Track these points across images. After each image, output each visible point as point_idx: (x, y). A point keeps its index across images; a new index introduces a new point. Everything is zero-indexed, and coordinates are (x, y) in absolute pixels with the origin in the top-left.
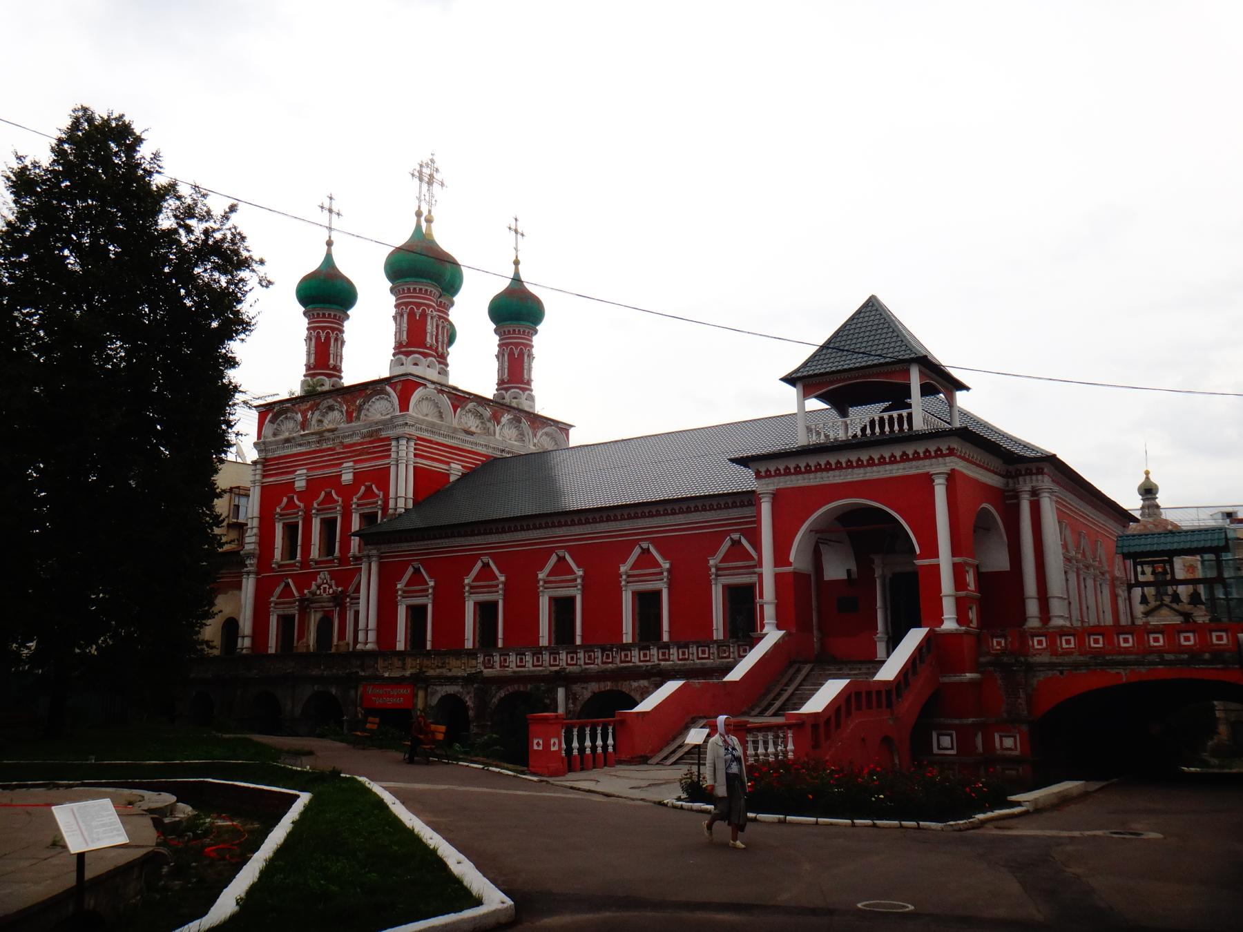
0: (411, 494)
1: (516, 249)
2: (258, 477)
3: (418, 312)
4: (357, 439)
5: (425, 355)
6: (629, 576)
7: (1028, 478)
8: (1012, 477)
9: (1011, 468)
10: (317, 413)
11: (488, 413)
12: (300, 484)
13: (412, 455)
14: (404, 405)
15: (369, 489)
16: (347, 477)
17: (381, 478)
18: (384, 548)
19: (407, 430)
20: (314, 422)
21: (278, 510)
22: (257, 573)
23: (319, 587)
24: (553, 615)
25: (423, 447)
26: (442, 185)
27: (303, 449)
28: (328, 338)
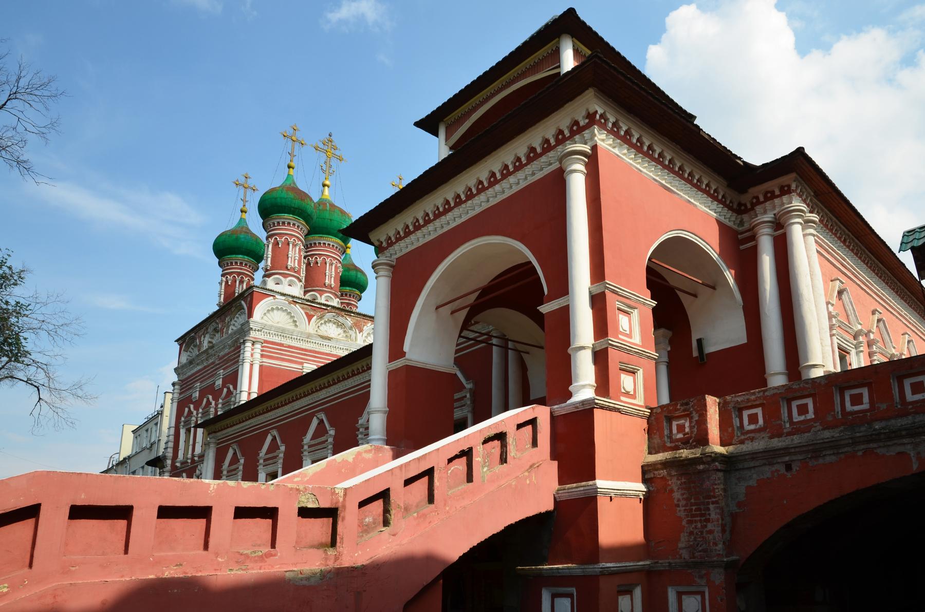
7: (768, 204)
8: (746, 211)
9: (746, 199)
13: (257, 356)
14: (250, 315)
15: (229, 388)
16: (219, 382)
18: (220, 434)
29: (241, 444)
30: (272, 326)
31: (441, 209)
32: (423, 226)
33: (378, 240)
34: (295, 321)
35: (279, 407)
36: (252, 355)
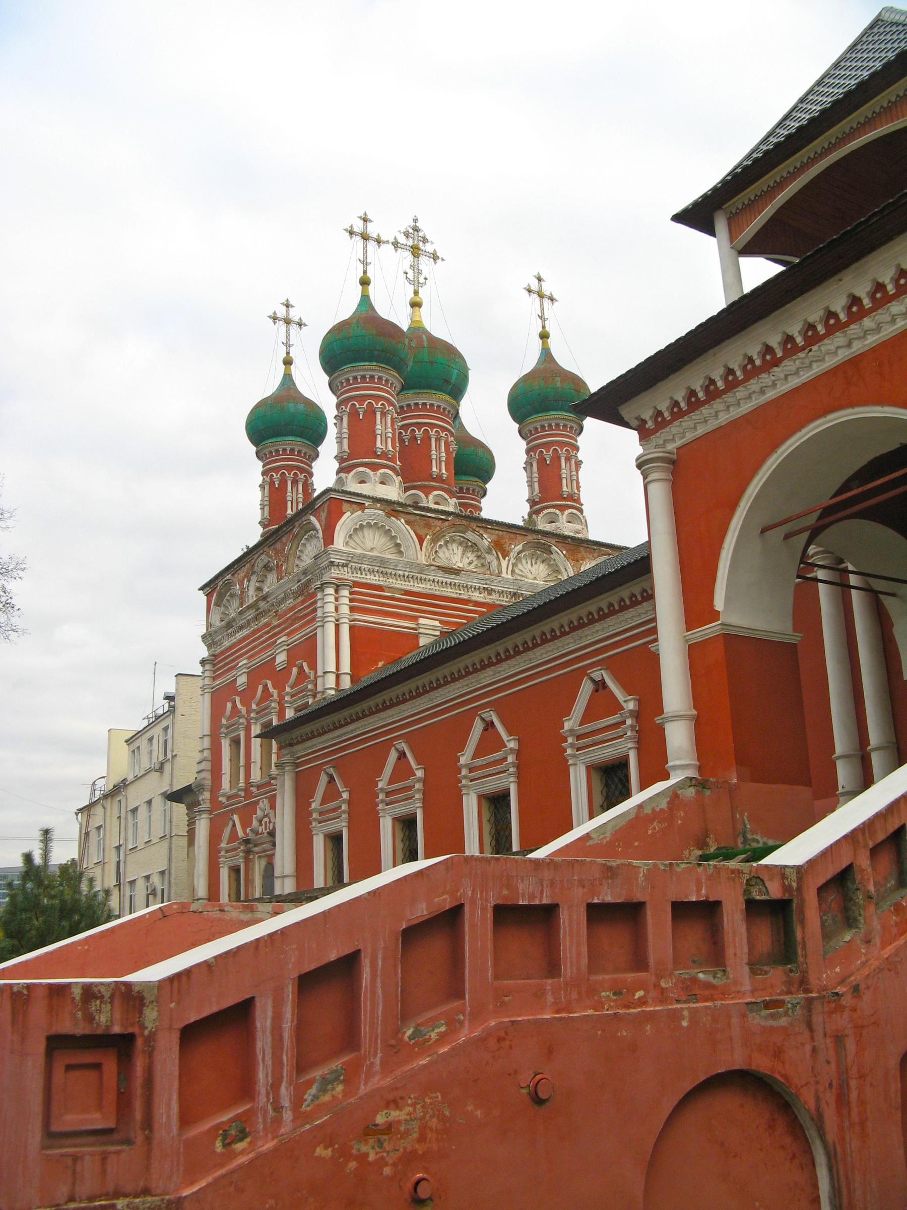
0: (346, 667)
1: (542, 317)
2: (207, 681)
3: (361, 408)
4: (290, 602)
5: (374, 467)
6: (579, 737)
10: (254, 578)
11: (486, 541)
12: (242, 680)
13: (345, 610)
14: (329, 539)
16: (281, 658)
17: (307, 651)
19: (334, 573)
20: (252, 592)
21: (224, 721)
22: (210, 812)
23: (260, 821)
24: (487, 827)
25: (364, 596)
26: (435, 257)
27: (245, 632)
28: (283, 482)
29: (336, 764)
30: (364, 556)
31: (758, 362)
32: (724, 392)
33: (638, 418)
34: (398, 545)
35: (404, 701)
36: (337, 609)
